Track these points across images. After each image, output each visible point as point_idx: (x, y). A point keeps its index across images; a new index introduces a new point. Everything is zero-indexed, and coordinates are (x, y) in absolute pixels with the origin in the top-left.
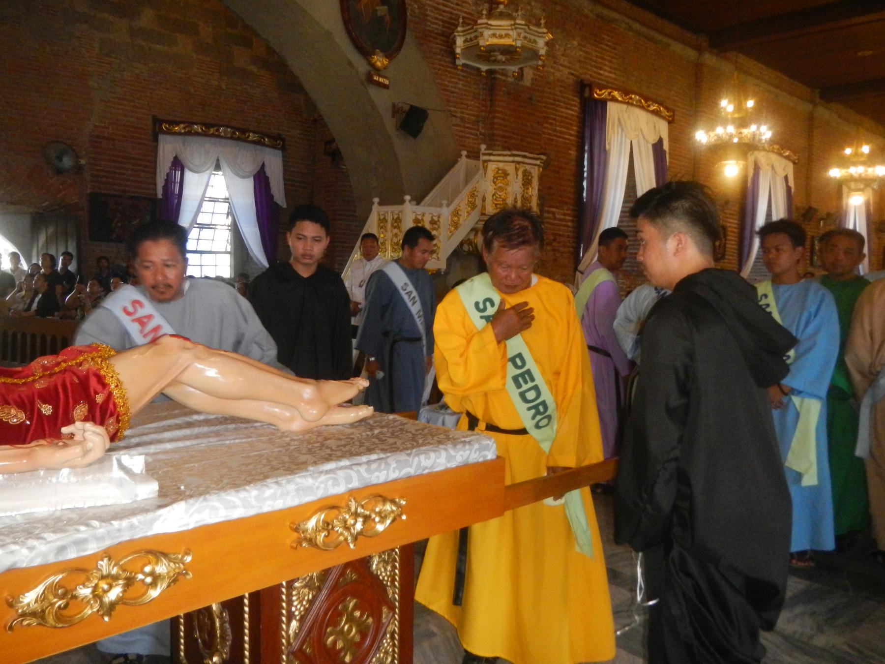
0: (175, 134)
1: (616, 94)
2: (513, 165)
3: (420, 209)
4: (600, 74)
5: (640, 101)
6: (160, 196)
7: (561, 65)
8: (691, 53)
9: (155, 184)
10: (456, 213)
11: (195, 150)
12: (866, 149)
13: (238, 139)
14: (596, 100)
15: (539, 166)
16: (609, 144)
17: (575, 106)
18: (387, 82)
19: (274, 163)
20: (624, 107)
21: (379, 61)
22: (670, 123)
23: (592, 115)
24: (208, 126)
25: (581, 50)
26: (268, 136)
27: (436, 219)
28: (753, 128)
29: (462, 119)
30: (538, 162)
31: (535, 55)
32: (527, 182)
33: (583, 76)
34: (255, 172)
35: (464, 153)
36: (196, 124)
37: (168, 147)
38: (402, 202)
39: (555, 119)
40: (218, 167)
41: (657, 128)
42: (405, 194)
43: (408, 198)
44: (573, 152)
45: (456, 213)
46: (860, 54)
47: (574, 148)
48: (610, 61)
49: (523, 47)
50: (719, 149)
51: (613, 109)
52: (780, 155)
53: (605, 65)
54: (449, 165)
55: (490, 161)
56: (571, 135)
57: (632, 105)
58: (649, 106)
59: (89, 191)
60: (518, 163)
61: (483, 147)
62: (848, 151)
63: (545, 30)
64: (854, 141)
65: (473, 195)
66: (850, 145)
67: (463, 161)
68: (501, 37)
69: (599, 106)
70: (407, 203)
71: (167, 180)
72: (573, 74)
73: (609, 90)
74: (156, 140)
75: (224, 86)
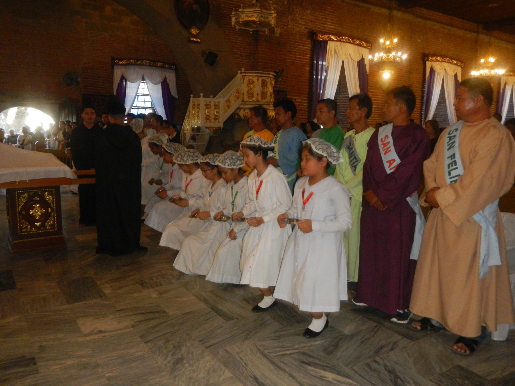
0: (122, 65)
1: (332, 37)
2: (256, 77)
3: (208, 100)
4: (324, 27)
5: (349, 40)
6: (115, 94)
7: (300, 24)
8: (385, 11)
9: (113, 89)
10: (228, 101)
11: (131, 72)
12: (492, 60)
13: (153, 66)
14: (321, 41)
15: (271, 78)
16: (328, 63)
17: (308, 44)
18: (199, 40)
19: (171, 77)
20: (339, 43)
21: (194, 31)
23: (319, 49)
24: (137, 60)
25: (313, 16)
26: (168, 64)
27: (217, 104)
28: (394, 53)
29: (241, 55)
30: (271, 76)
31: (268, 24)
32: (264, 84)
33: (314, 28)
34: (162, 80)
36: (132, 59)
38: (199, 97)
39: (296, 52)
40: (143, 79)
41: (360, 53)
42: (192, 93)
43: (202, 94)
44: (307, 68)
45: (228, 101)
46: (490, 5)
47: (308, 66)
48: (331, 20)
49: (260, 22)
50: (381, 64)
51: (331, 45)
52: (451, 63)
53: (328, 22)
54: (232, 77)
55: (246, 76)
56: (306, 59)
57: (343, 42)
58: (355, 42)
59: (82, 93)
60: (258, 76)
61: (243, 69)
62: (482, 61)
63: (273, 12)
64: (485, 55)
65: (237, 92)
67: (239, 75)
68: (250, 17)
69: (323, 44)
70: (202, 97)
71: (118, 87)
72: (307, 28)
73: (327, 36)
74: (113, 68)
75: (145, 40)
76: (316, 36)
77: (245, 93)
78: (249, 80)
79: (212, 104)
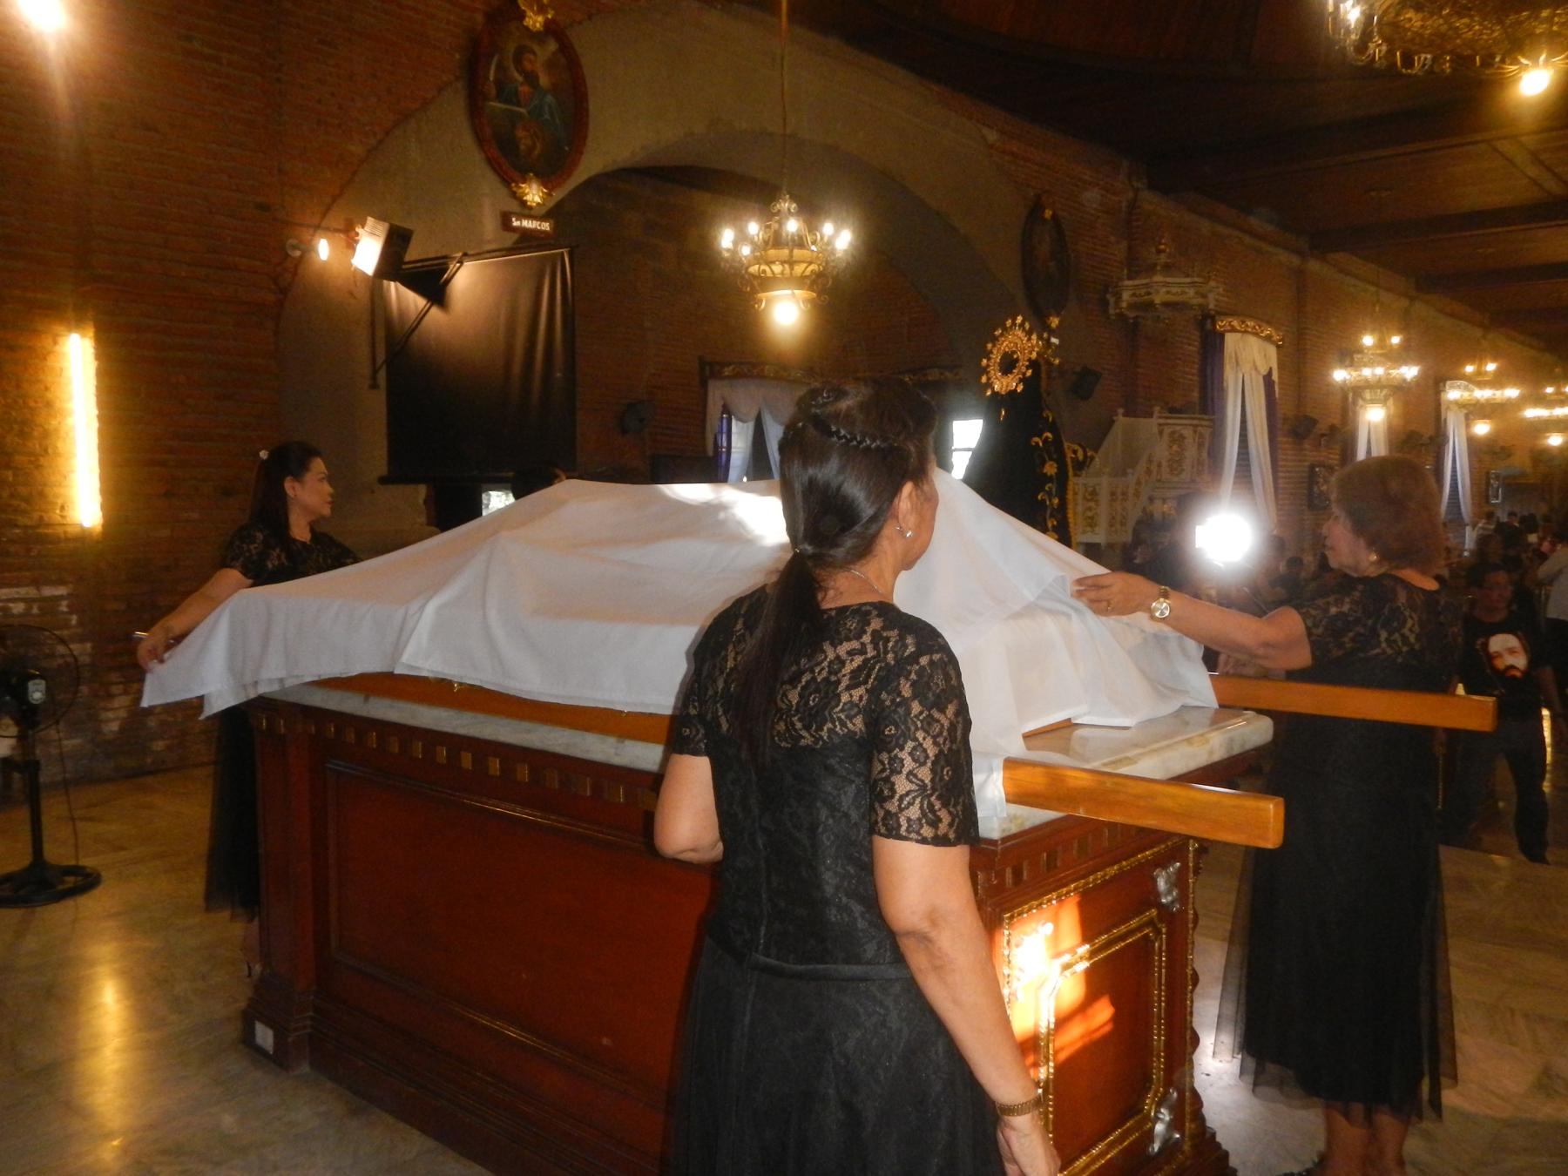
0: (729, 377)
6: (711, 453)
8: (1296, 261)
12: (1491, 367)
22: (1278, 347)
35: (1121, 411)
37: (717, 393)
44: (1196, 394)
50: (1356, 391)
51: (1231, 340)
62: (1469, 369)
64: (1477, 356)
65: (1150, 461)
66: (1472, 360)
67: (1121, 420)
74: (704, 385)
76: (1214, 324)
77: (1164, 464)
78: (1173, 433)
79: (1119, 491)
